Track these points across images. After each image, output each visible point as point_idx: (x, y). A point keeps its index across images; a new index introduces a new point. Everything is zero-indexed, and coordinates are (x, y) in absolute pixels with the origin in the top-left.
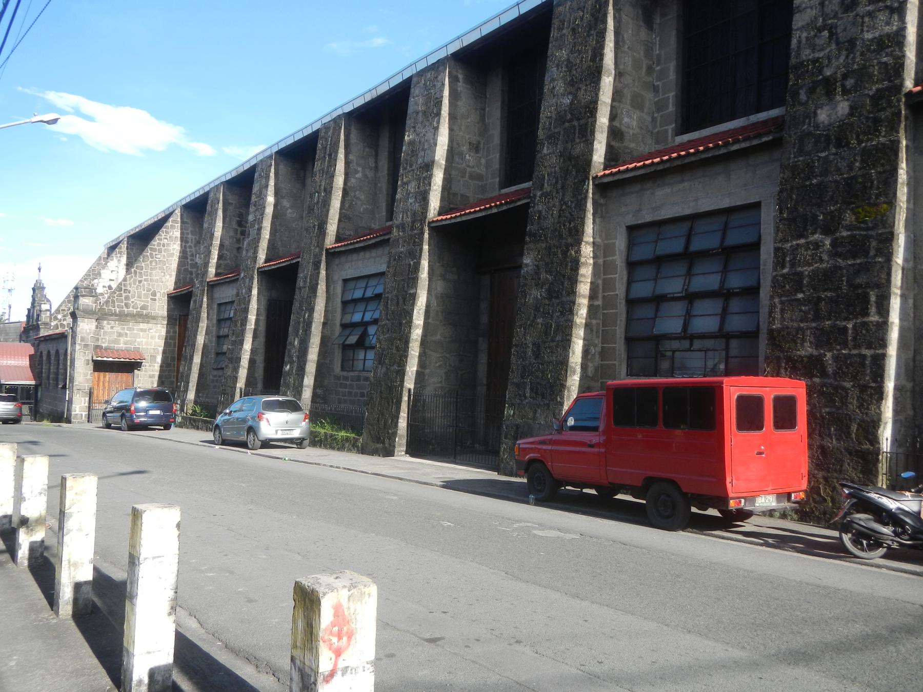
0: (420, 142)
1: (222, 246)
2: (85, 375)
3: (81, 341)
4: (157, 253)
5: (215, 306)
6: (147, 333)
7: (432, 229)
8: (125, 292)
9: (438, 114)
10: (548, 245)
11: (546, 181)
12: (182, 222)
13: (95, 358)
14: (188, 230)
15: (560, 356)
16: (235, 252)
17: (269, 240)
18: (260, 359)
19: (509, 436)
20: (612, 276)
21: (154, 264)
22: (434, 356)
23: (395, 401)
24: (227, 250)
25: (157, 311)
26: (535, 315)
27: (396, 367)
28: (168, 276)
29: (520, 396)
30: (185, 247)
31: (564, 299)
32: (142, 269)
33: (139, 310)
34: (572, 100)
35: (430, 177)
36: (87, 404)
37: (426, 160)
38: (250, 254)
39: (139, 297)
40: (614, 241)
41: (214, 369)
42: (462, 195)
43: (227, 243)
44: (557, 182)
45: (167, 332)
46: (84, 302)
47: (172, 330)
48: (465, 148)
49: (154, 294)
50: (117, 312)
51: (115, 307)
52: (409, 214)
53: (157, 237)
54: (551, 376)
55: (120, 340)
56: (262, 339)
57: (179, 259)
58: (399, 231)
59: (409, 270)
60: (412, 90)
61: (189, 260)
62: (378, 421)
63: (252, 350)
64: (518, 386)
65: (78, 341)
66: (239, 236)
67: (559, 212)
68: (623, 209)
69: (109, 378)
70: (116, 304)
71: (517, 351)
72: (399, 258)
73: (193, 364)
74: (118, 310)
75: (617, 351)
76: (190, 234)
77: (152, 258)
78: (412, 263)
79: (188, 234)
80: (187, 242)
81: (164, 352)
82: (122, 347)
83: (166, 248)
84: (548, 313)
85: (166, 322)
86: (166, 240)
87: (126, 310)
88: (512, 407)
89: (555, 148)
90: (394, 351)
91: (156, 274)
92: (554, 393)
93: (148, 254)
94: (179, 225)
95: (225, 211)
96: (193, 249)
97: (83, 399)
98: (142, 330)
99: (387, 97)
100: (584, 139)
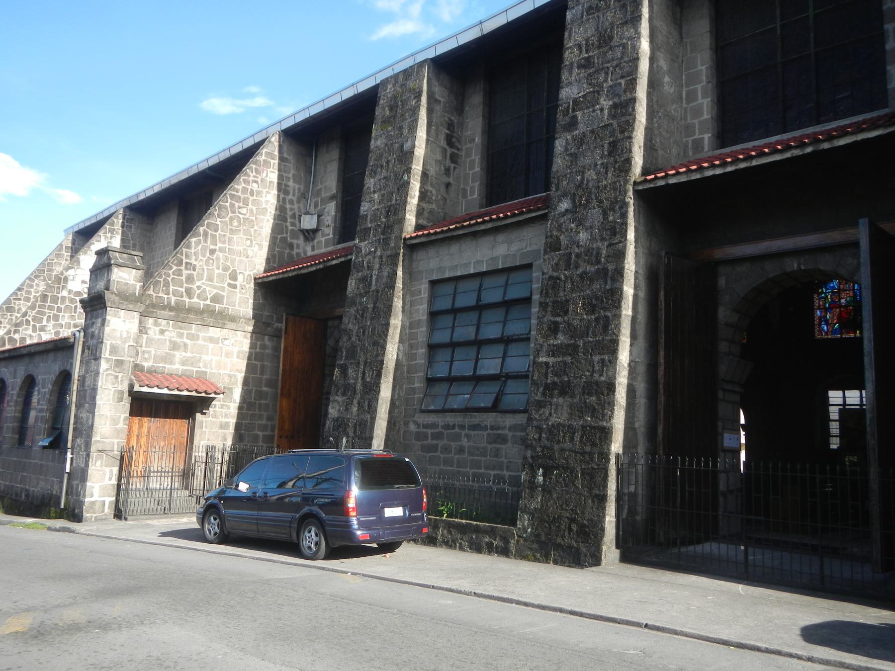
1: (425, 175)
2: (115, 421)
3: (111, 353)
4: (241, 204)
5: (424, 288)
6: (220, 345)
8: (186, 268)
12: (282, 159)
13: (137, 388)
14: (289, 173)
16: (443, 189)
17: (646, 128)
18: (641, 387)
21: (235, 223)
24: (432, 185)
25: (237, 308)
28: (257, 247)
30: (284, 199)
32: (216, 231)
33: (208, 302)
36: (114, 481)
38: (595, 156)
39: (210, 279)
41: (423, 411)
43: (432, 172)
45: (252, 346)
46: (120, 277)
47: (259, 343)
49: (234, 276)
50: (173, 303)
51: (168, 294)
53: (241, 178)
55: (174, 356)
56: (641, 342)
57: (274, 219)
61: (288, 224)
63: (629, 365)
65: (106, 353)
66: (448, 162)
69: (149, 428)
70: (171, 288)
73: (380, 401)
74: (173, 300)
76: (291, 180)
77: (233, 212)
79: (288, 179)
80: (286, 193)
81: (246, 382)
82: (178, 369)
83: (255, 197)
85: (250, 329)
86: (255, 185)
87: (187, 300)
91: (239, 242)
93: (228, 204)
94: (277, 161)
95: (430, 111)
96: (296, 206)
97: (107, 470)
98: (212, 340)
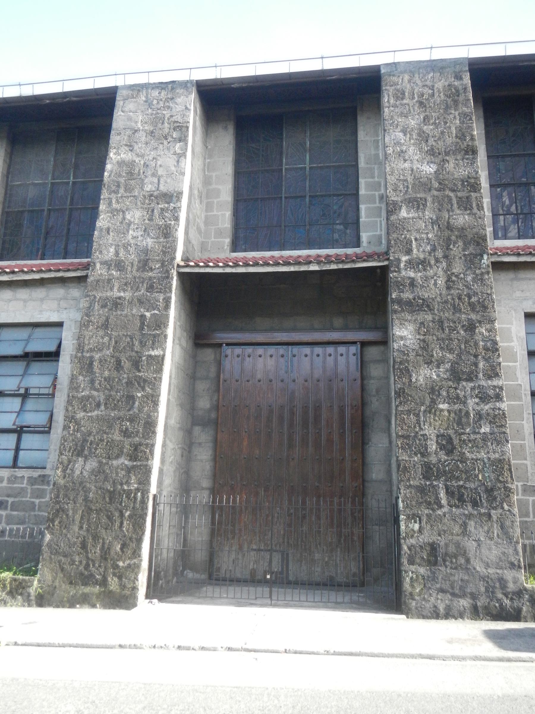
0: (146, 165)
7: (181, 275)
9: (183, 139)
10: (437, 318)
11: (414, 246)
15: (494, 452)
19: (418, 560)
20: (510, 364)
22: (170, 445)
23: (127, 514)
26: (432, 399)
27: (124, 461)
29: (429, 503)
31: (483, 383)
34: (438, 170)
35: (176, 210)
37: (162, 188)
40: (508, 326)
42: (193, 247)
44: (434, 249)
48: (196, 192)
52: (132, 250)
54: (483, 476)
58: (109, 269)
59: (142, 324)
60: (119, 103)
62: (84, 546)
64: (421, 490)
67: (446, 282)
68: (518, 294)
71: (408, 444)
72: (117, 304)
75: (527, 448)
78: (148, 314)
84: (458, 397)
88: (413, 518)
89: (420, 213)
90: (117, 437)
92: (495, 499)
99: (48, 101)
100: (468, 212)
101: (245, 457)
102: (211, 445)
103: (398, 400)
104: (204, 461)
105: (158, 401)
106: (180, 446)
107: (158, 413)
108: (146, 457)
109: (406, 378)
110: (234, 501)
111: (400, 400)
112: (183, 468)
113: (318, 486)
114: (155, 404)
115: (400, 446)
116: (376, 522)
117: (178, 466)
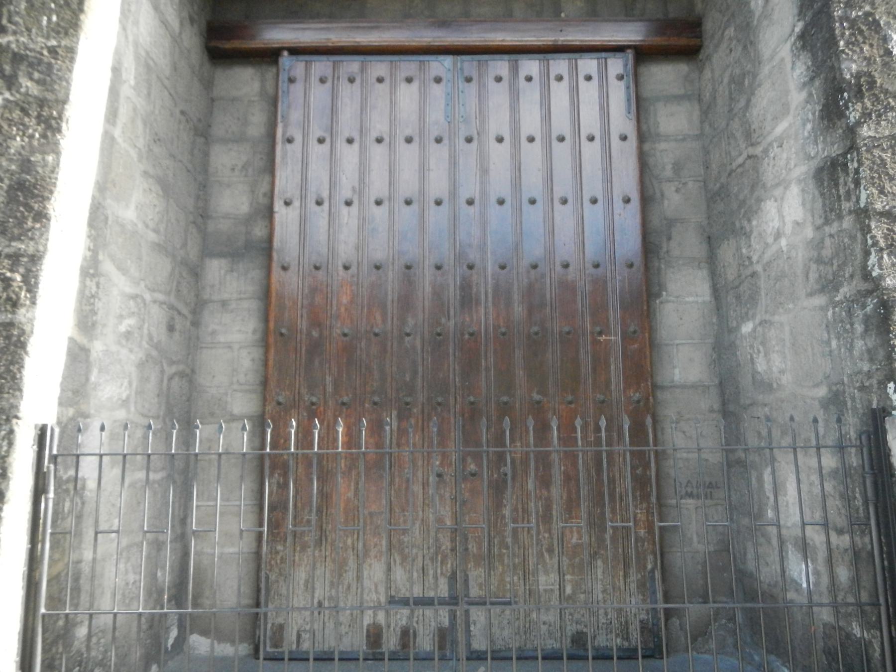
101: (346, 331)
102: (253, 305)
103: (859, 106)
104: (236, 347)
105: (60, 117)
106: (161, 297)
107: (58, 153)
108: (9, 299)
109: (871, 46)
110: (329, 438)
111: (864, 108)
112: (172, 363)
113: (538, 402)
114: (49, 127)
115: (882, 244)
116: (689, 490)
117: (154, 353)
